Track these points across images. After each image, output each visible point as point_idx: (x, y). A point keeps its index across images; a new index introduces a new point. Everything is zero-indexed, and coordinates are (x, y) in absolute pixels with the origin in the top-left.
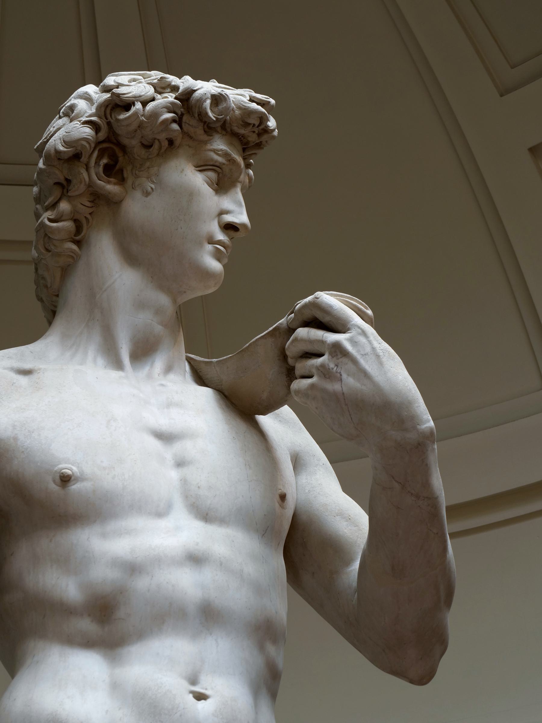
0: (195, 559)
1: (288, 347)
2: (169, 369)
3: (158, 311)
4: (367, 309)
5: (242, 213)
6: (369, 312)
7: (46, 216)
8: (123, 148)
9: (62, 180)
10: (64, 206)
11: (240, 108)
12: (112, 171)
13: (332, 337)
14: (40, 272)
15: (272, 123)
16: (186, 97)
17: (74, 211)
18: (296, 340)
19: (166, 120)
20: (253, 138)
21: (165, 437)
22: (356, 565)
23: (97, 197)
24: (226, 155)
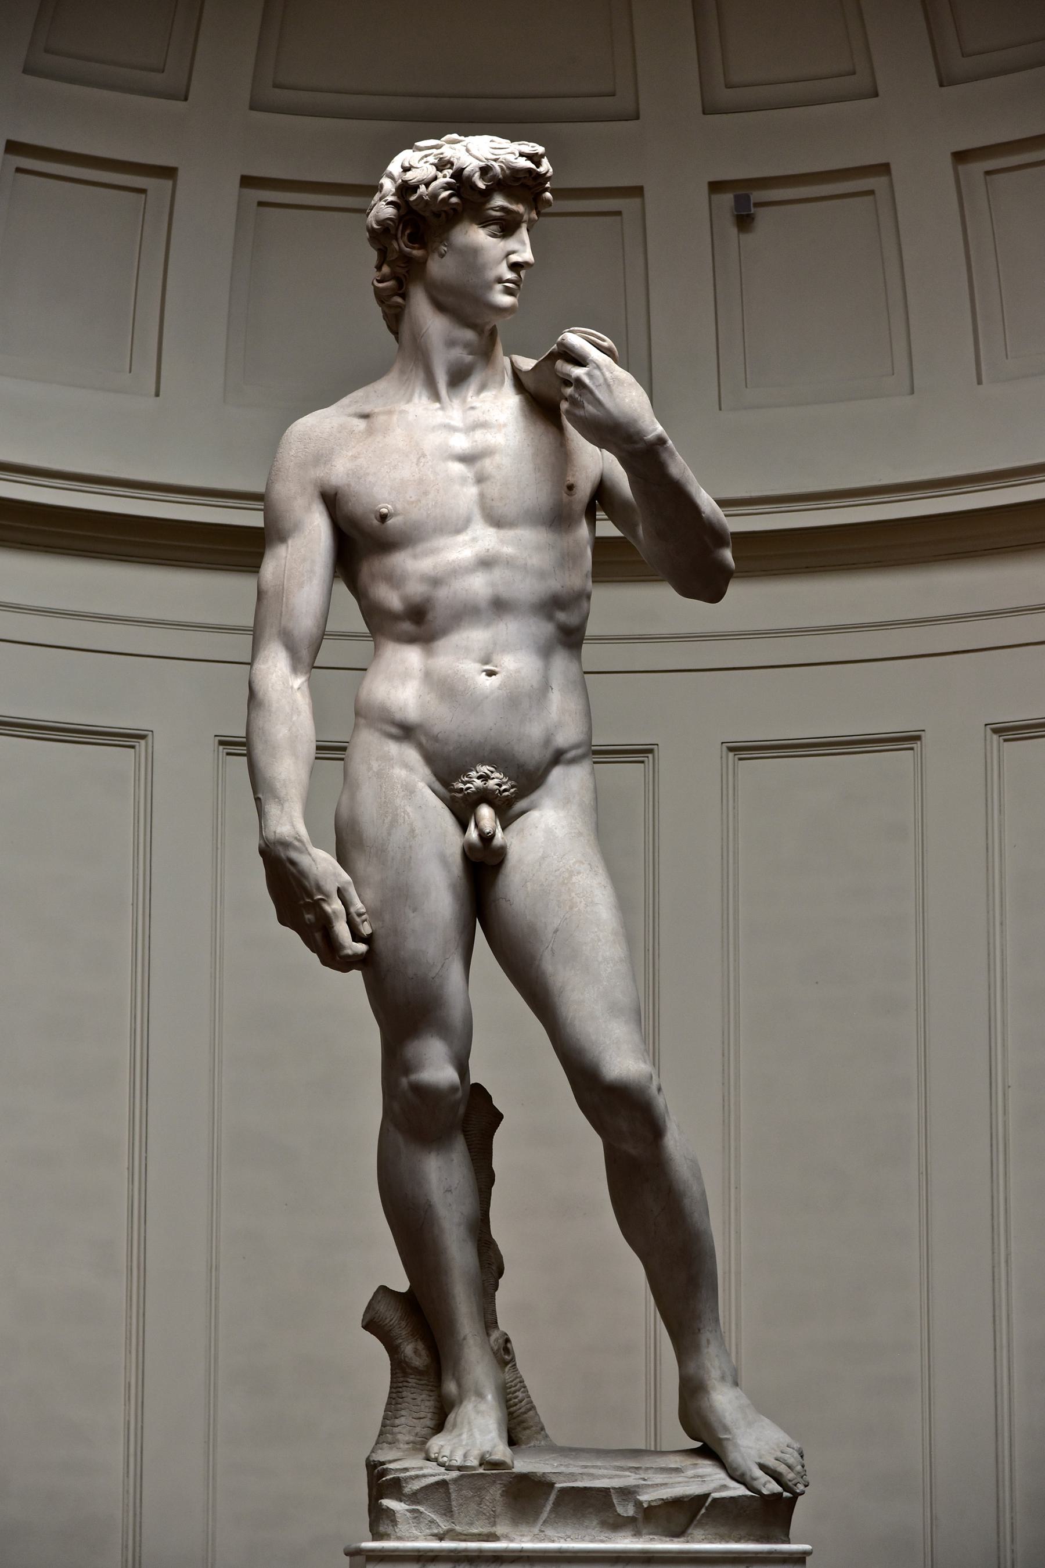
0: (486, 563)
2: (483, 387)
3: (467, 346)
4: (604, 340)
5: (525, 251)
8: (423, 218)
10: (386, 269)
11: (508, 168)
15: (546, 166)
16: (459, 174)
19: (444, 199)
20: (530, 183)
21: (467, 459)
22: (641, 528)
23: (408, 259)
24: (502, 209)
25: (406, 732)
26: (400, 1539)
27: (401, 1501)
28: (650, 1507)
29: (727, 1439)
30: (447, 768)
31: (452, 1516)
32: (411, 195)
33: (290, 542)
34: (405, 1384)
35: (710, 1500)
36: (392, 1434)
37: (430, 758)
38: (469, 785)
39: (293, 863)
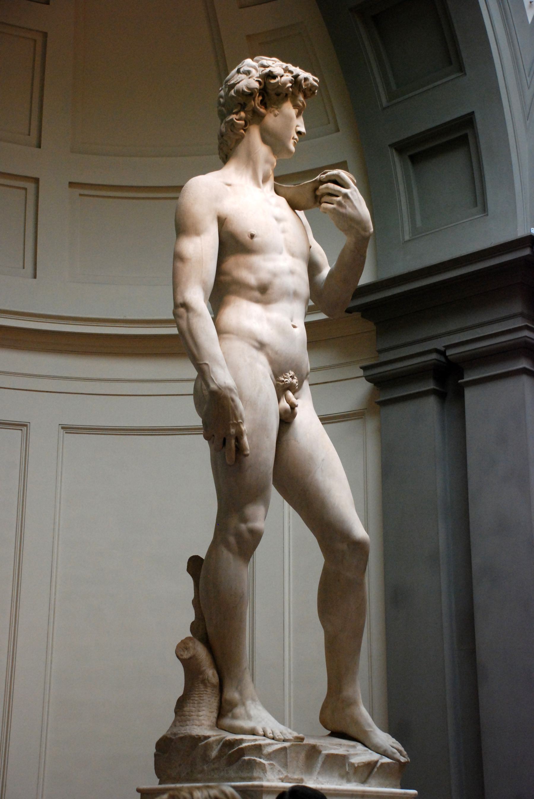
0: (292, 272)
1: (322, 189)
6: (355, 181)
7: (234, 117)
9: (242, 103)
10: (243, 114)
12: (263, 103)
13: (344, 190)
14: (225, 138)
16: (296, 77)
17: (246, 117)
18: (327, 188)
25: (261, 346)
26: (268, 781)
27: (260, 758)
28: (358, 766)
29: (371, 731)
30: (278, 369)
31: (287, 768)
32: (271, 79)
33: (202, 236)
34: (205, 692)
35: (379, 764)
36: (199, 720)
37: (272, 362)
38: (286, 380)
39: (233, 400)
